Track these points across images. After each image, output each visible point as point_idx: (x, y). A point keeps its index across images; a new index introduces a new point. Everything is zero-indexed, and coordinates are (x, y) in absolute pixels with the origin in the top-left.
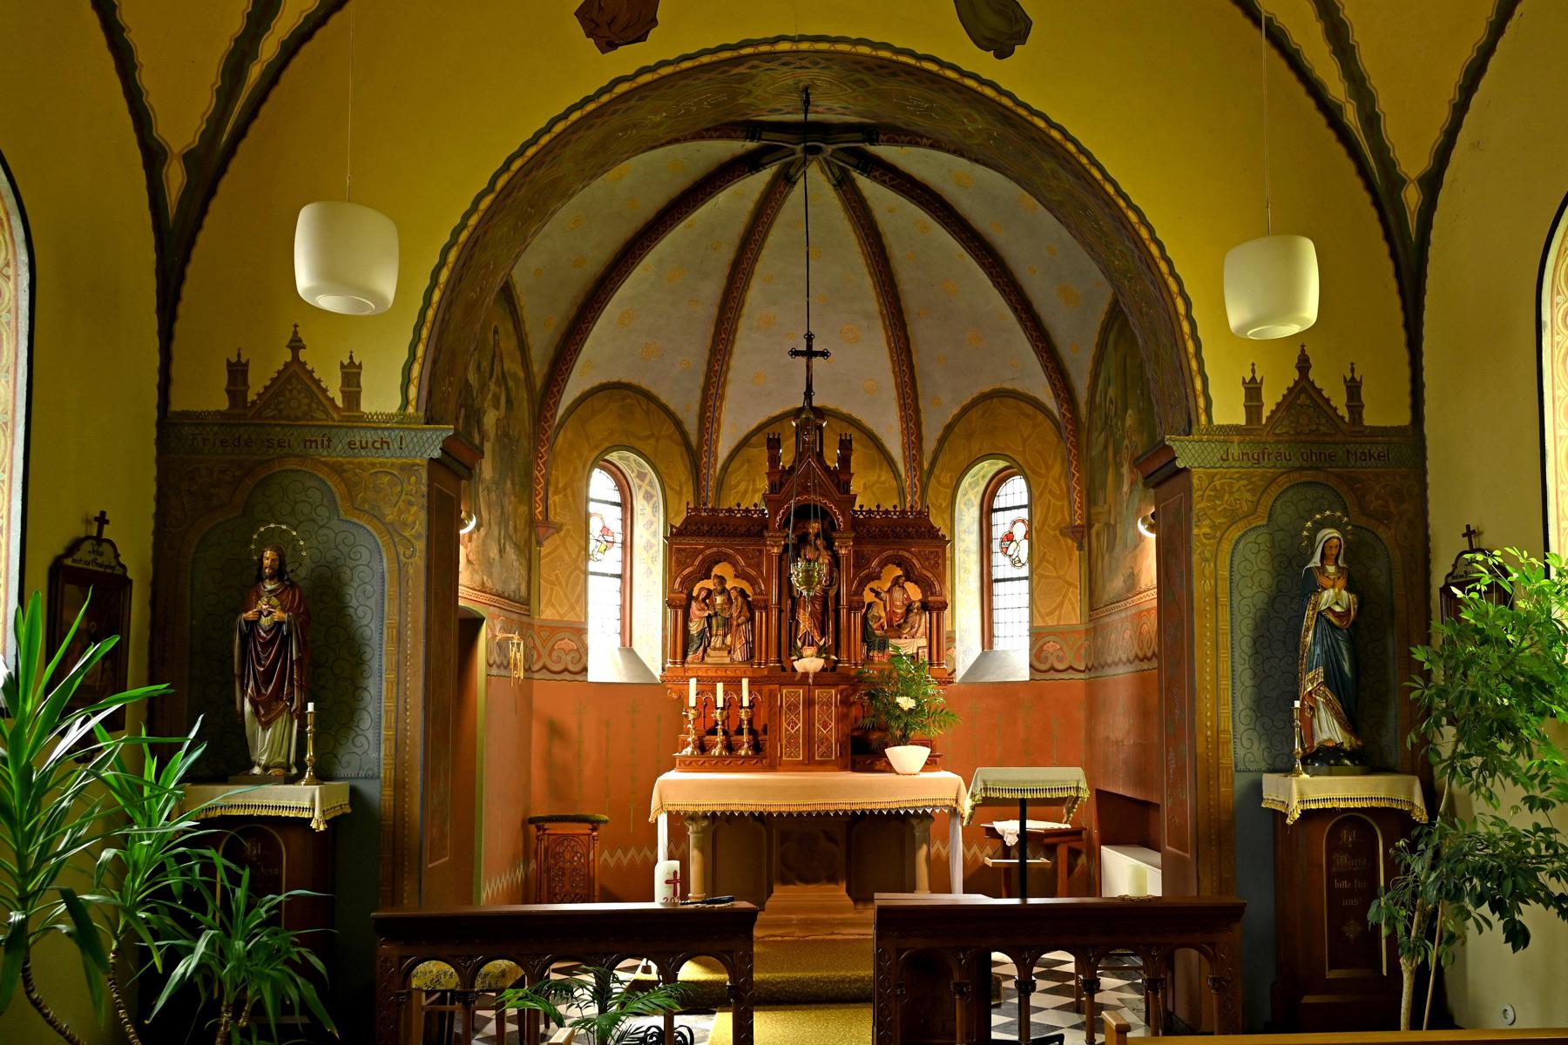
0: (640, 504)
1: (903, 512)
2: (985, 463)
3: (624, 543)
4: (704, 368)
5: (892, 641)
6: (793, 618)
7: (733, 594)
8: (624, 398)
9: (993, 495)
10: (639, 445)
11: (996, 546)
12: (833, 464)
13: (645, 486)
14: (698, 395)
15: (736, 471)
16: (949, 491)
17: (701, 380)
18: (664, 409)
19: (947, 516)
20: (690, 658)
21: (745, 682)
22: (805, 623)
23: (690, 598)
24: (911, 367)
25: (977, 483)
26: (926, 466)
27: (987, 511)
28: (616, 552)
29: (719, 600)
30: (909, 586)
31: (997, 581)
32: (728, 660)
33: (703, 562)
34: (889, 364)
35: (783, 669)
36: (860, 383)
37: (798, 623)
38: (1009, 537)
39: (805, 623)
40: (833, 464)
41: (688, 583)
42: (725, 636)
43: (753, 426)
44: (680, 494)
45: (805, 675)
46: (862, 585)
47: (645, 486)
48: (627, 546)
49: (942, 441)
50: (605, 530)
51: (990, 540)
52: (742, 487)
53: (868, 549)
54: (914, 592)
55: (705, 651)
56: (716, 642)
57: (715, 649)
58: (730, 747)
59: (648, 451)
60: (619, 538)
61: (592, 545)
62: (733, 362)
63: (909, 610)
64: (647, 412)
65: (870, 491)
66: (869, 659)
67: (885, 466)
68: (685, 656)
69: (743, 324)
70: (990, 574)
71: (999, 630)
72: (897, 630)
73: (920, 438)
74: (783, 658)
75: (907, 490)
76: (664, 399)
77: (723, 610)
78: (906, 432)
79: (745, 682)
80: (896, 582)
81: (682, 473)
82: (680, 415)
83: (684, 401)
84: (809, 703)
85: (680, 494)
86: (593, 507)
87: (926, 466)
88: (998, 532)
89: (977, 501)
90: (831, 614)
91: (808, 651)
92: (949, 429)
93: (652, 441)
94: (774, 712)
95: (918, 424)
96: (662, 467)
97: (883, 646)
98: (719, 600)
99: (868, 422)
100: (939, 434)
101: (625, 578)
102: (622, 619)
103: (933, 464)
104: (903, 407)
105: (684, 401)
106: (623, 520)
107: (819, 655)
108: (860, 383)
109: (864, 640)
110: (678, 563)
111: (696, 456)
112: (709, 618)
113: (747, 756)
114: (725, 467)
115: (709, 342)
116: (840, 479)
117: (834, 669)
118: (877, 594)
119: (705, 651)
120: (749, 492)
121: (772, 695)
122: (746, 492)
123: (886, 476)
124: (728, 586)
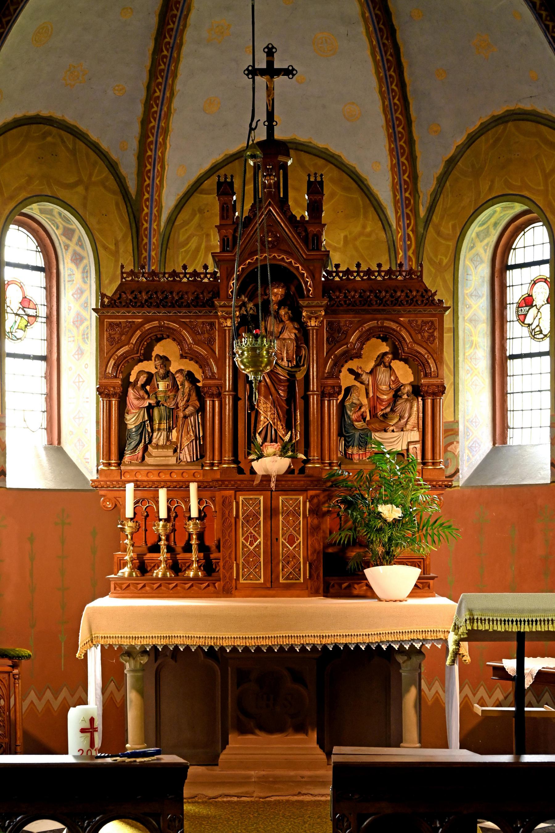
0: (67, 268)
1: (390, 272)
2: (497, 208)
3: (49, 318)
4: (143, 94)
5: (376, 436)
6: (252, 407)
7: (179, 378)
8: (45, 135)
9: (508, 247)
10: (62, 194)
11: (511, 313)
12: (301, 212)
13: (73, 245)
14: (137, 129)
15: (186, 223)
16: (452, 244)
17: (140, 109)
18: (95, 148)
19: (449, 277)
20: (127, 458)
21: (193, 487)
22: (266, 414)
23: (126, 384)
24: (402, 85)
25: (487, 233)
26: (422, 212)
27: (500, 267)
28: (39, 329)
29: (162, 386)
30: (397, 365)
31: (513, 357)
32: (173, 461)
33: (141, 339)
34: (374, 82)
35: (240, 471)
36: (335, 107)
37: (258, 414)
38: (528, 302)
39: (266, 414)
40: (301, 212)
41: (124, 365)
42: (169, 430)
43: (207, 166)
44: (115, 254)
45: (267, 478)
46: (338, 364)
47: (73, 245)
48: (53, 321)
49: (442, 180)
50: (26, 302)
51: (504, 305)
52: (193, 244)
53: (344, 319)
54: (404, 374)
55: (145, 449)
56: (159, 438)
57: (157, 446)
58: (176, 567)
59: (75, 202)
60: (43, 311)
61: (10, 321)
62: (178, 86)
63: (397, 396)
64: (73, 152)
65: (348, 245)
66: (347, 457)
67: (371, 212)
68: (121, 455)
69: (189, 35)
70: (503, 348)
71: (513, 419)
72: (382, 421)
73: (414, 177)
74: (241, 457)
75: (399, 244)
76: (94, 136)
77: (167, 398)
78: (397, 168)
79: (193, 487)
80: (380, 360)
81: (119, 228)
82: (114, 156)
83: (119, 138)
84: (272, 512)
85: (115, 254)
86: (9, 273)
87: (422, 212)
88: (514, 295)
89: (487, 256)
90: (299, 402)
91: (270, 448)
92: (451, 163)
93: (80, 189)
94: (230, 525)
95: (412, 158)
96: (92, 222)
97: (364, 443)
98: (162, 386)
99: (350, 158)
100: (439, 170)
101: (52, 360)
102: (49, 411)
103: (431, 210)
104: (393, 137)
105: (119, 138)
106: (48, 289)
107: (283, 453)
108: (335, 107)
109: (340, 434)
110: (111, 340)
111: (135, 208)
112: (150, 408)
113: (196, 578)
114: (172, 220)
115: (148, 63)
116: (309, 234)
117: (302, 471)
118: (357, 376)
119: (145, 449)
120: (197, 251)
121: (226, 503)
122: (197, 250)
123: (372, 225)
124: (173, 369)
